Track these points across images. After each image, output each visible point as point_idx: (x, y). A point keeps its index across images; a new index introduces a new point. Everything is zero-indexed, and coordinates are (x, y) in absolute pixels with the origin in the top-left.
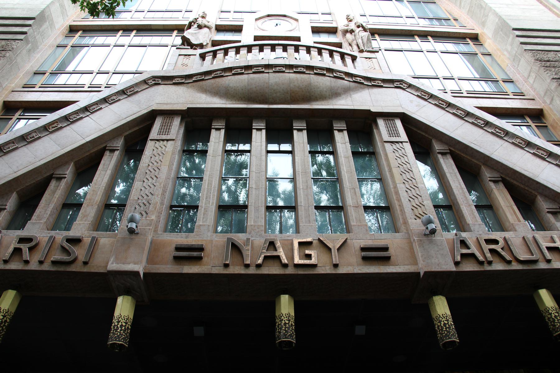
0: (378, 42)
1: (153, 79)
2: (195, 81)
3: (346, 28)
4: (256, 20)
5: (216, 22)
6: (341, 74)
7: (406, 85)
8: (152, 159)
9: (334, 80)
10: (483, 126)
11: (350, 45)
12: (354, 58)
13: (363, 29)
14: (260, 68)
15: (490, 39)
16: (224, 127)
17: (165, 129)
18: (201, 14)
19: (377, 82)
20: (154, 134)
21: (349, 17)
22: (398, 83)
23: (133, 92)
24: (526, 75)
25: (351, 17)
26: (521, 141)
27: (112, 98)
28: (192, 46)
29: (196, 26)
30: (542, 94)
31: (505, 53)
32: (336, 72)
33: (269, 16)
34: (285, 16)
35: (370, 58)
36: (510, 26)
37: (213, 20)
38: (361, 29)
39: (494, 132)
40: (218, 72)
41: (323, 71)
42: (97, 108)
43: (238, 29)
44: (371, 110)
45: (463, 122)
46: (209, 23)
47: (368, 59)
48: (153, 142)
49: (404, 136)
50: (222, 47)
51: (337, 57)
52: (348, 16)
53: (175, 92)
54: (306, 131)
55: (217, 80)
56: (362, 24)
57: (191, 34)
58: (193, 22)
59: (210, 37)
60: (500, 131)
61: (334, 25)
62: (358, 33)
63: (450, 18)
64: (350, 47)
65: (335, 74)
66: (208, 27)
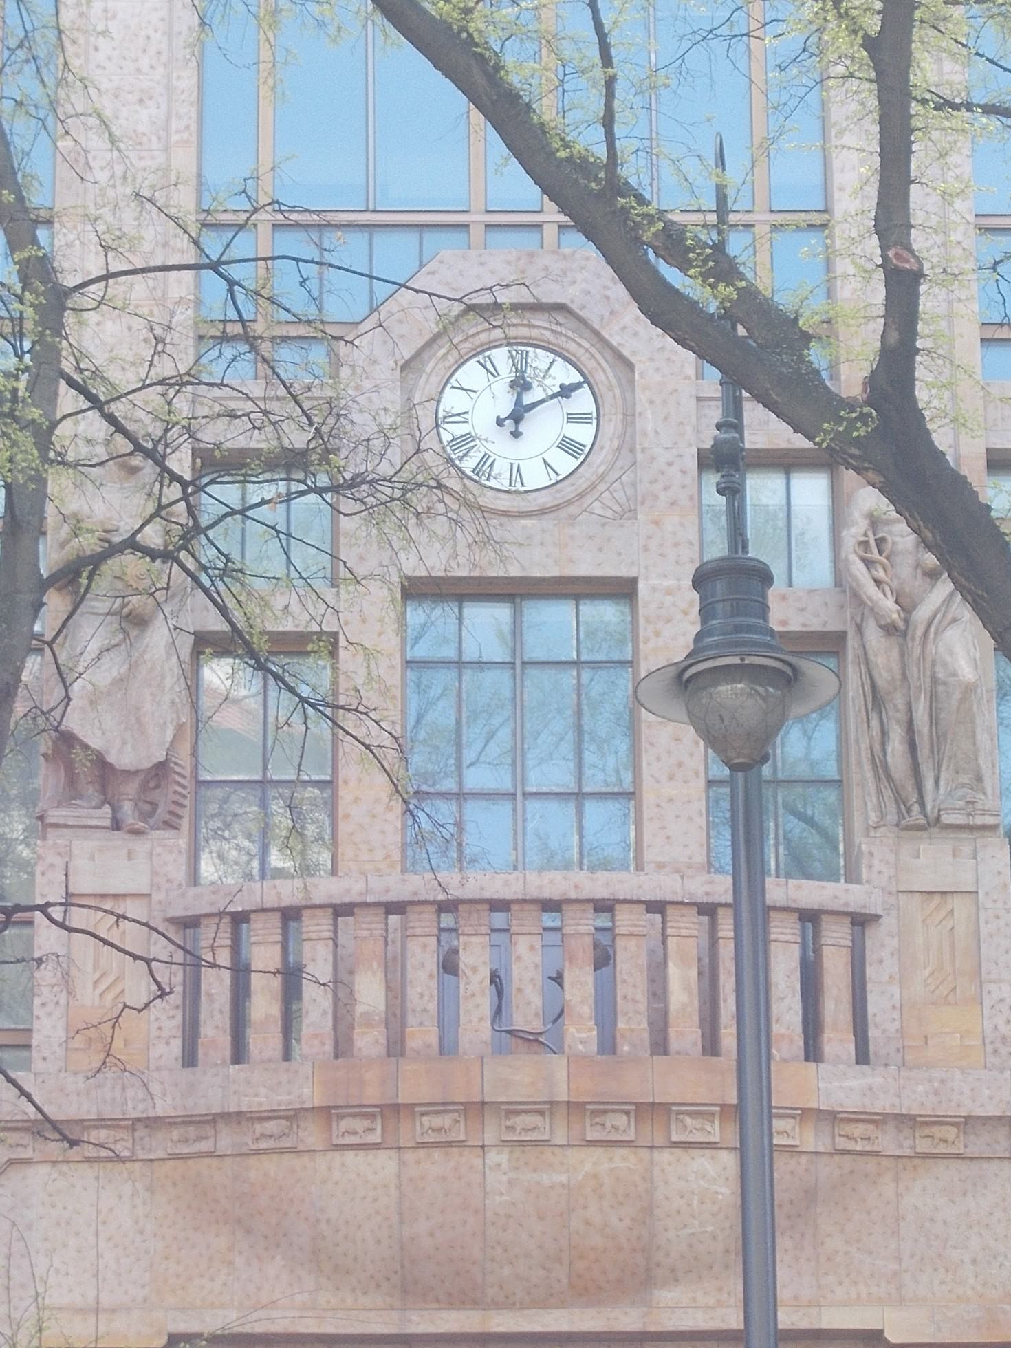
14: (446, 1121)
19: (938, 1131)
40: (271, 1127)
41: (709, 1128)
44: (887, 1335)
47: (937, 899)
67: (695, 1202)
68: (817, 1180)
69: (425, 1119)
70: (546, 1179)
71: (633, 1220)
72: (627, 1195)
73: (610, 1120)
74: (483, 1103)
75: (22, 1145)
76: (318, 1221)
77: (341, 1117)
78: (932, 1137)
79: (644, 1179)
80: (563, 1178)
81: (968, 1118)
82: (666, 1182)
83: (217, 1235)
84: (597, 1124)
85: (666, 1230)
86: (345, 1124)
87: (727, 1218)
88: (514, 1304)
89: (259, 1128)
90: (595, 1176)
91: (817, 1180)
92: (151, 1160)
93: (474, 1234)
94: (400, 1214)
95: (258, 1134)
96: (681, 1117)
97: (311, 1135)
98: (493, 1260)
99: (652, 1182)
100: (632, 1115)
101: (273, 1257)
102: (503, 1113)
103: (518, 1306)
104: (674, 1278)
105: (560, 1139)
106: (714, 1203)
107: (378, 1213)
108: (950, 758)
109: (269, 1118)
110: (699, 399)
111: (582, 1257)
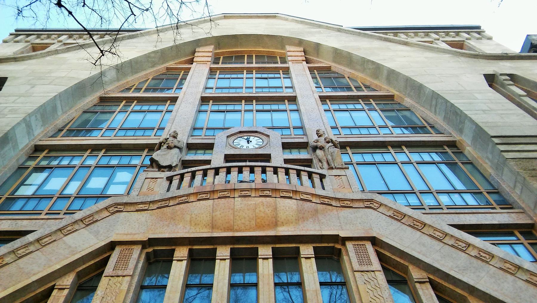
0: (349, 155)
1: (115, 206)
2: (158, 208)
3: (315, 144)
4: (228, 137)
5: (187, 140)
6: (307, 196)
7: (377, 205)
8: (104, 300)
9: (301, 202)
10: (464, 249)
11: (320, 161)
12: (322, 177)
13: (333, 144)
14: (226, 193)
15: (469, 146)
16: (186, 258)
17: (123, 261)
18: (172, 134)
19: (346, 202)
20: (109, 269)
21: (319, 132)
22: (369, 203)
23: (93, 221)
24: (512, 185)
25: (321, 132)
26: (510, 267)
27: (69, 229)
28: (160, 168)
29: (165, 146)
30: (532, 207)
31: (487, 161)
32: (302, 194)
33: (241, 132)
34: (256, 132)
35: (339, 176)
36: (488, 134)
37: (183, 138)
38: (330, 144)
39: (478, 256)
42: (50, 241)
43: (209, 147)
44: (340, 235)
45: (442, 244)
46: (180, 143)
47: (338, 177)
48: (107, 278)
49: (376, 265)
50: (190, 170)
51: (305, 177)
52: (319, 131)
53: (138, 220)
54: (271, 260)
55: (182, 206)
56: (331, 140)
57: (160, 156)
58: (163, 142)
59: (180, 158)
60: (484, 255)
61: (304, 140)
62: (328, 148)
63: (426, 125)
64: (320, 163)
65: (302, 197)
66: (178, 148)
67: (287, 208)
68: (317, 208)
69: (220, 193)
70: (250, 203)
71: (272, 211)
72: (270, 206)
73: (265, 192)
74: (235, 189)
75: (121, 208)
76: (192, 214)
77: (200, 195)
78: (344, 203)
79: (274, 203)
80: (254, 203)
81: (352, 199)
82: (280, 204)
83: (166, 222)
84: (262, 193)
85: (280, 213)
86: (200, 196)
87: (295, 212)
88: (241, 230)
89: (180, 199)
90: (262, 202)
91: (317, 208)
92: (152, 210)
93: (231, 214)
94: (213, 211)
95: (179, 200)
96: (283, 192)
97: (192, 199)
98: (236, 219)
99: (276, 203)
100: (271, 191)
101: (180, 224)
102: (239, 191)
103: (242, 231)
104: (283, 224)
105: (253, 195)
106: (292, 209)
107: (207, 211)
108: (336, 162)
109: (183, 197)
110: (281, 138)
111: (259, 218)
